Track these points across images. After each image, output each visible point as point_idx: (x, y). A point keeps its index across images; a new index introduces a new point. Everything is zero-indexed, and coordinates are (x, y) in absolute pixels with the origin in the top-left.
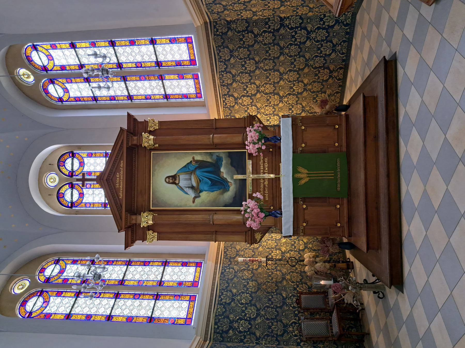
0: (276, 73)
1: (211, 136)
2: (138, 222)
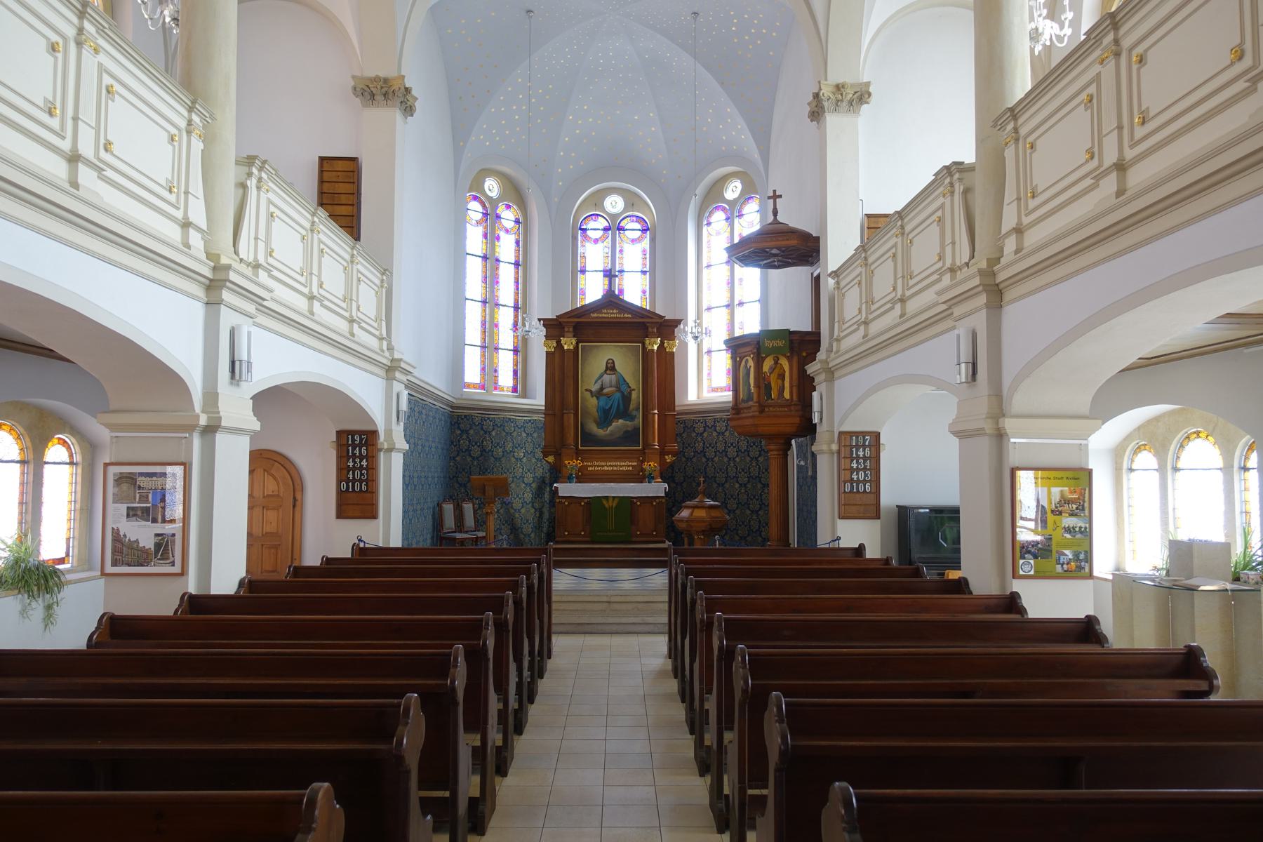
0: (724, 479)
1: (656, 412)
2: (566, 334)
